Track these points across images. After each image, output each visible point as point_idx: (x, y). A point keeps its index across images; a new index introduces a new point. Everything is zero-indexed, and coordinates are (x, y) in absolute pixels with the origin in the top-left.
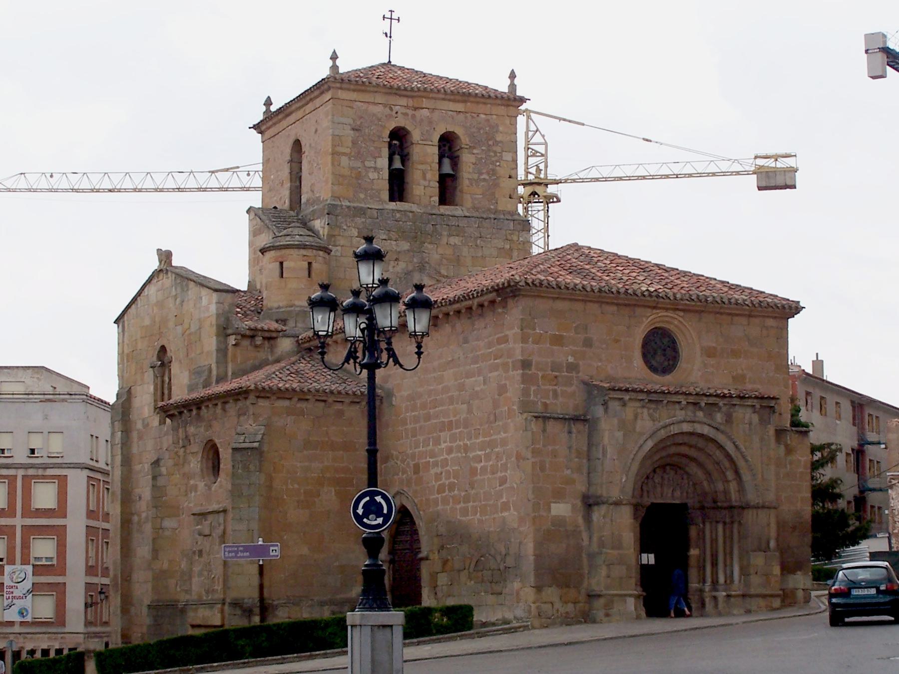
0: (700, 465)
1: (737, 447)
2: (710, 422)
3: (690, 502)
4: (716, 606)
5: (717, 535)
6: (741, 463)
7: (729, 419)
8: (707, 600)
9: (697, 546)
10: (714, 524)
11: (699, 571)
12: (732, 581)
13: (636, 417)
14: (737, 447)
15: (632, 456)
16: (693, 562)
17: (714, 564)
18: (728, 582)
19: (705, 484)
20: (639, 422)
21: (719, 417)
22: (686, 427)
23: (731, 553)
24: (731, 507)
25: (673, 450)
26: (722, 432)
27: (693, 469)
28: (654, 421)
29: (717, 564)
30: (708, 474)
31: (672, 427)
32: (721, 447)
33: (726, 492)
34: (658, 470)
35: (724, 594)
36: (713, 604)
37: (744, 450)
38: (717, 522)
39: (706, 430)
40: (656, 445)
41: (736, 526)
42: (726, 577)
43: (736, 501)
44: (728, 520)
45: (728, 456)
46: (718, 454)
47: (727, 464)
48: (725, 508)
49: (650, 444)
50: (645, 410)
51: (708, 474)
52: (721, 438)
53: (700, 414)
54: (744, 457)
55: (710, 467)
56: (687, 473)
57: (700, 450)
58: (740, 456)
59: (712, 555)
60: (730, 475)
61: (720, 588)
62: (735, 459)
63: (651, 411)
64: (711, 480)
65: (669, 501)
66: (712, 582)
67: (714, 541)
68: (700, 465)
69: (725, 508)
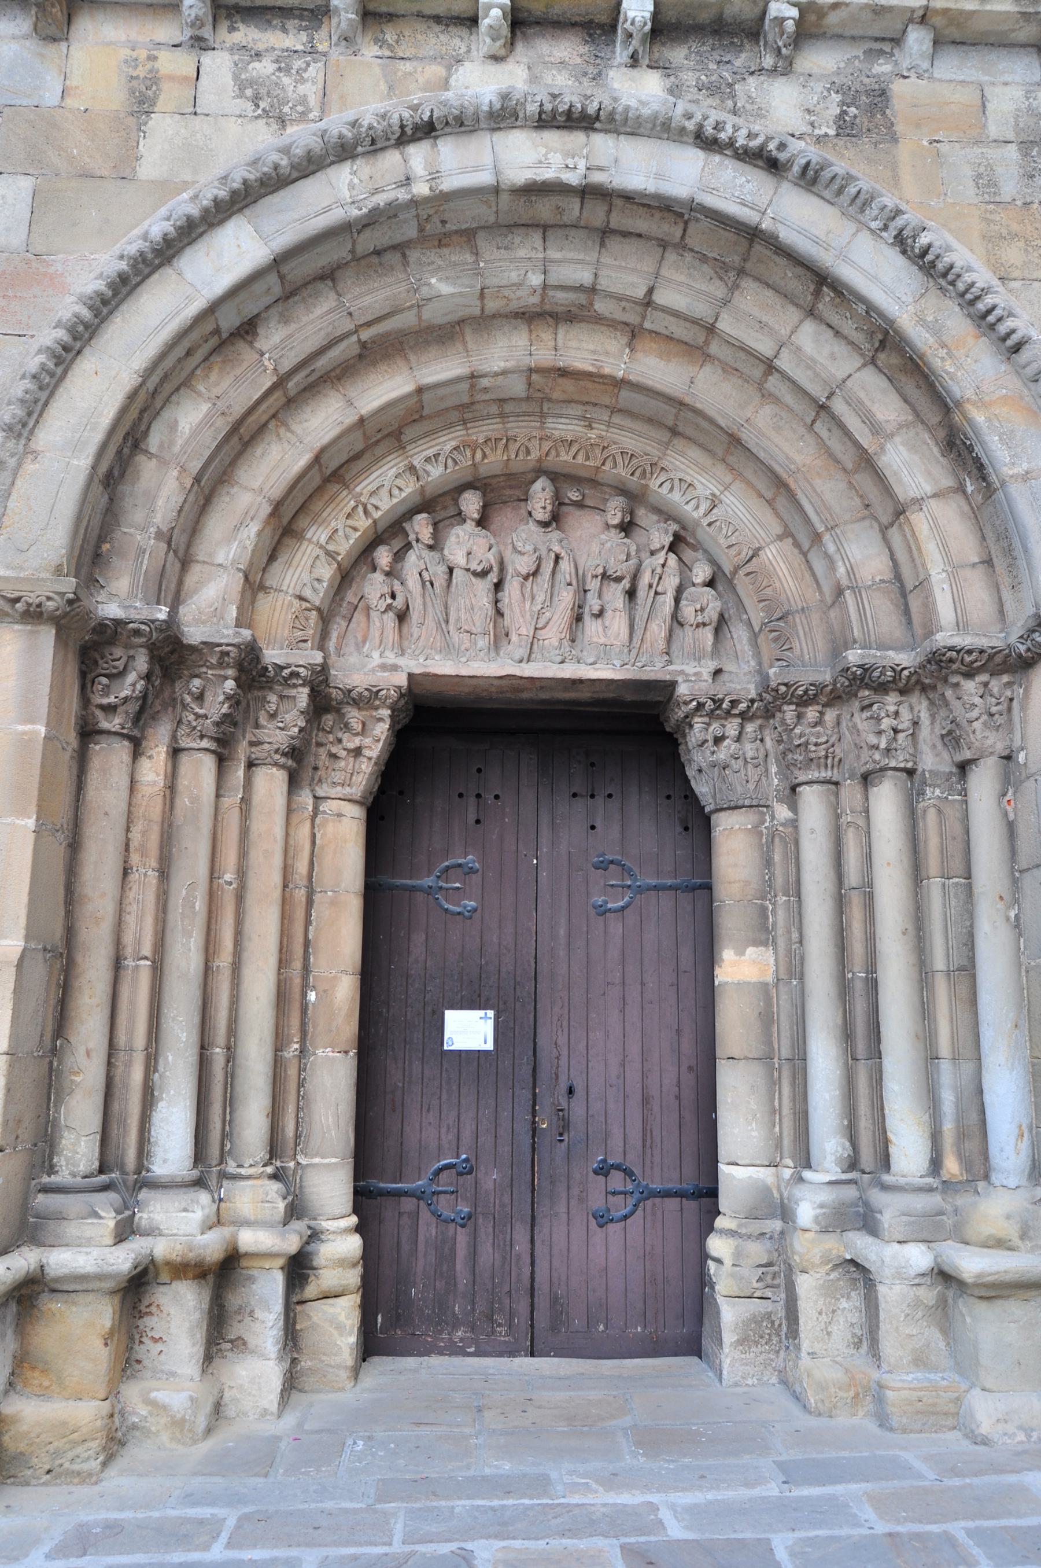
0: (730, 447)
1: (927, 264)
2: (710, 113)
3: (691, 677)
4: (869, 1337)
5: (868, 857)
6: (971, 370)
7: (867, 113)
8: (806, 1285)
9: (763, 934)
10: (850, 792)
11: (773, 1084)
12: (980, 1169)
13: (143, 102)
14: (927, 264)
15: (70, 307)
16: (735, 1025)
17: (862, 1041)
18: (952, 1166)
19: (778, 559)
20: (163, 129)
21: (785, 106)
22: (528, 157)
23: (967, 971)
24: (941, 669)
25: (504, 354)
26: (810, 178)
27: (692, 485)
28: (282, 121)
29: (876, 1053)
30: (778, 488)
31: (418, 155)
32: (820, 287)
33: (905, 589)
34: (471, 503)
35: (919, 1257)
36: (850, 1305)
37: (981, 276)
38: (867, 779)
39: (680, 173)
40: (278, 262)
41: (983, 783)
42: (936, 1138)
43: (962, 625)
44: (932, 760)
45: (885, 345)
46: (817, 353)
47: (879, 400)
48: (902, 684)
49: (236, 252)
50: (218, 66)
51: (778, 488)
52: (797, 217)
53: (640, 89)
54: (985, 321)
55: (787, 445)
56: (665, 514)
57: (699, 341)
58: (956, 323)
59: (844, 989)
60: (912, 465)
61: (891, 1210)
62: (920, 337)
63: (265, 67)
64: (806, 538)
65: (529, 670)
66: (853, 1164)
67: (852, 898)
68: (730, 447)
69: (902, 684)
